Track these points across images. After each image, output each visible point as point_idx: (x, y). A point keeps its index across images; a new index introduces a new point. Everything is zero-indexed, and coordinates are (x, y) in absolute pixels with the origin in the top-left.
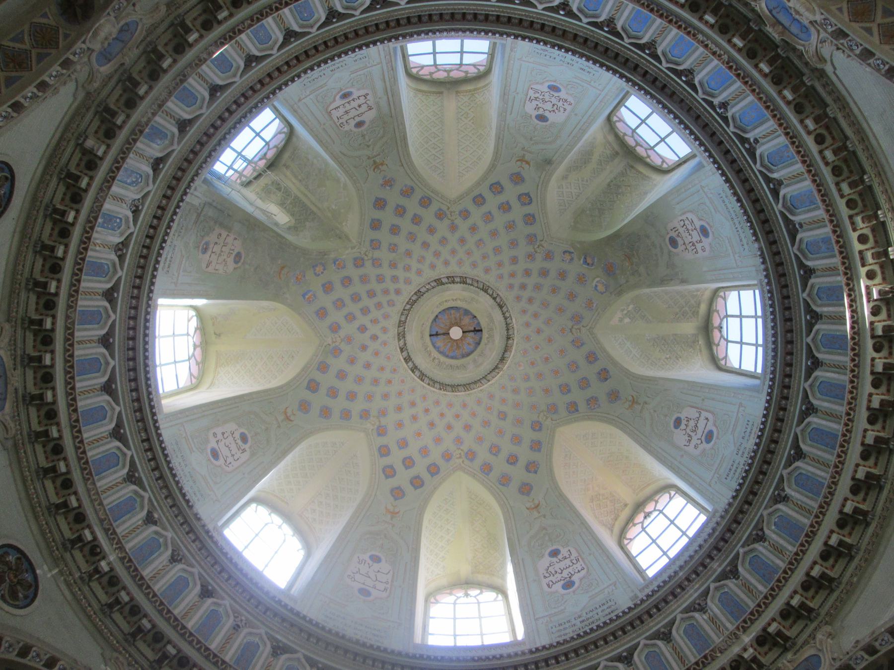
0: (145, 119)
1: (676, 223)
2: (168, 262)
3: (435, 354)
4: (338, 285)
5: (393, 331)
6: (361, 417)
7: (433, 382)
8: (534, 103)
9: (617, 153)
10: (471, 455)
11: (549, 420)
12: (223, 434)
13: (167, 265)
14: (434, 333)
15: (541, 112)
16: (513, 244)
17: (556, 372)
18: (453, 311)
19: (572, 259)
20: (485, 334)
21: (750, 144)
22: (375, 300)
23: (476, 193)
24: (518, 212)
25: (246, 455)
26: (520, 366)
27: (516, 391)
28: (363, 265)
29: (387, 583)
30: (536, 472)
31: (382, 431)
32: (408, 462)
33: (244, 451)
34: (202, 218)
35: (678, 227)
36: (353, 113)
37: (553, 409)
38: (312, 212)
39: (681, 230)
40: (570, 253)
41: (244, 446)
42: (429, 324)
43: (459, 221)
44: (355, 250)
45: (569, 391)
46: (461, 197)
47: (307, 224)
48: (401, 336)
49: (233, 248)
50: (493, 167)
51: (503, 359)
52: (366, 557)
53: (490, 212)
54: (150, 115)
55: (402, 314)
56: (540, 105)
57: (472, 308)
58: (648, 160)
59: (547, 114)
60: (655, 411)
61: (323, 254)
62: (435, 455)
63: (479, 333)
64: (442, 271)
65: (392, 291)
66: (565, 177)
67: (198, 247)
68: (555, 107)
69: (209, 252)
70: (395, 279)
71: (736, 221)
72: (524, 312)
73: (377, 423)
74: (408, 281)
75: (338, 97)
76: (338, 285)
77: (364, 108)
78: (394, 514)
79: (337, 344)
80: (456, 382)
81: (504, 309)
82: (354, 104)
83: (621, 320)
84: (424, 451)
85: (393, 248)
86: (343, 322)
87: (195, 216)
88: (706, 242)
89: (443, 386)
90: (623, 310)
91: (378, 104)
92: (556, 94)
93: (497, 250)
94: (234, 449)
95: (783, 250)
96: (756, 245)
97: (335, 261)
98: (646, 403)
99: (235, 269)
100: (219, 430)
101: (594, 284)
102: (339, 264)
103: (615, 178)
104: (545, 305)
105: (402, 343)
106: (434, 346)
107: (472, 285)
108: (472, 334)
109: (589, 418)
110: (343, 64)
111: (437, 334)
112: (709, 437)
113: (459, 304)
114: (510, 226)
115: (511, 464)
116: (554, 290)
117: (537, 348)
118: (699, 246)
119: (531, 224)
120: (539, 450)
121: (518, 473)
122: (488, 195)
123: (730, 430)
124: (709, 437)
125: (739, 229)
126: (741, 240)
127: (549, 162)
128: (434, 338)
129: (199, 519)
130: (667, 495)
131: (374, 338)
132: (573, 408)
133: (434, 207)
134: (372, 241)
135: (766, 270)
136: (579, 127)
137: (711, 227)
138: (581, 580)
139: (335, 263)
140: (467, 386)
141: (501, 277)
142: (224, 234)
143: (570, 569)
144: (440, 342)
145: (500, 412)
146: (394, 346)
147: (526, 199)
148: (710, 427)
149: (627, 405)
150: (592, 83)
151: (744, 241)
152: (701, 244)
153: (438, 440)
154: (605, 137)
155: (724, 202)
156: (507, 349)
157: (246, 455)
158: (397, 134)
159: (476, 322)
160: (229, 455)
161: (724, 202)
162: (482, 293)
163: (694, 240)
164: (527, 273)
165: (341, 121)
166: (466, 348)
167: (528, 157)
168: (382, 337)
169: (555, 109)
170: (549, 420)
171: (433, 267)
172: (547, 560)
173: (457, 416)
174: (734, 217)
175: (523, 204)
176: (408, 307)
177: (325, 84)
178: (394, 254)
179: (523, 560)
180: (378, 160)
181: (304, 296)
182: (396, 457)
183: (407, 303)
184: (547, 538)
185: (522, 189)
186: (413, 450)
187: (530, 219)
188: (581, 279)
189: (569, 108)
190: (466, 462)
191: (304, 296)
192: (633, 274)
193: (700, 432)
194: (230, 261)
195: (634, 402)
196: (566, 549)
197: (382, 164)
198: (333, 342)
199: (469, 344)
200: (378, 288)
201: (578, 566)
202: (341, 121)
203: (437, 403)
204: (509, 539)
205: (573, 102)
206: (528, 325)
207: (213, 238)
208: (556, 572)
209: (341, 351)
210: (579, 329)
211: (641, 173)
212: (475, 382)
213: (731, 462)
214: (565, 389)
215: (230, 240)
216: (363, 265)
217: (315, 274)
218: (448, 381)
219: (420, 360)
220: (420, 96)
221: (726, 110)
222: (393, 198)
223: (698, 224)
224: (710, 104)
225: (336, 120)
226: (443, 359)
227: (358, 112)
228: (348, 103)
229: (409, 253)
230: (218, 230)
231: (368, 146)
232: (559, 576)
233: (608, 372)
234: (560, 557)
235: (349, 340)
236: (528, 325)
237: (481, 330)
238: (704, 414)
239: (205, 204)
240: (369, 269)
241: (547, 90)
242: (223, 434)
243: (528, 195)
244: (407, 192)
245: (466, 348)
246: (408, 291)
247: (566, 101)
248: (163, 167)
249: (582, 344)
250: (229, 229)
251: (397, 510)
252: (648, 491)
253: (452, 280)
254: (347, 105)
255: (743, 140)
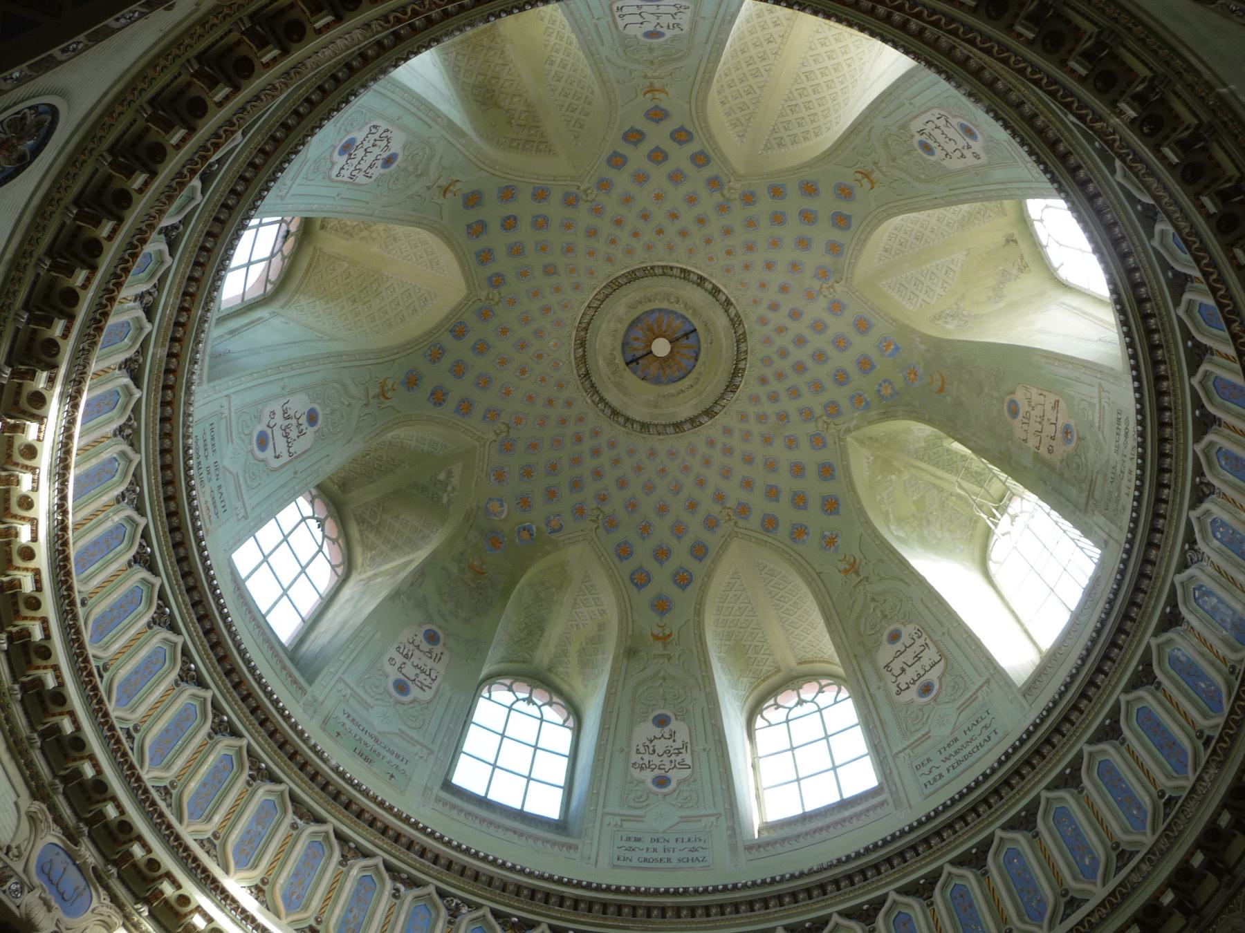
0: (1212, 771)
1: (440, 668)
2: (1123, 426)
3: (678, 308)
4: (853, 370)
5: (749, 323)
6: (753, 194)
7: (666, 271)
8: (678, 744)
9: (549, 670)
10: (571, 201)
11: (483, 298)
12: (963, 156)
13: (1123, 426)
14: (691, 336)
15: (666, 730)
16: (632, 506)
17: (503, 362)
18: (678, 374)
19: (548, 523)
20: (620, 361)
21: (403, 882)
22: (791, 360)
23: (708, 560)
24: (643, 555)
25: (917, 125)
26: (556, 345)
27: (547, 310)
28: (826, 407)
29: (622, 16)
30: (469, 227)
31: (715, 183)
32: (658, 156)
33: (921, 132)
34: (1085, 486)
35: (434, 665)
36: (909, 656)
37: (485, 314)
38: (921, 460)
39: (430, 663)
40: (554, 531)
41: (923, 138)
42: (703, 346)
43: (715, 509)
44: (844, 427)
45: (474, 348)
46: (724, 547)
47: (923, 445)
48: (736, 322)
49: (1025, 427)
50: (699, 612)
51: (582, 343)
52: (669, 34)
53: (679, 538)
54: (1206, 777)
55: (746, 352)
56: (670, 742)
57: (649, 391)
58: (508, 682)
59: (657, 731)
60: (350, 405)
61: (888, 415)
62: (622, 180)
63: (629, 359)
64: (711, 428)
65: (771, 379)
66: (601, 627)
67: (1079, 438)
68: (651, 749)
69: (1060, 424)
70: (774, 398)
71: (370, 742)
72: (580, 419)
73: (725, 192)
74: (755, 399)
75: (937, 686)
76: (853, 370)
77: (896, 666)
78: (651, 89)
79: (825, 286)
80: (634, 285)
81: (608, 411)
82: (911, 673)
83: (450, 474)
84: (641, 178)
85: (792, 443)
86: (827, 317)
87: (1097, 494)
88: (394, 674)
89: (649, 272)
90: (454, 489)
91: (880, 678)
92: (657, 772)
93: (649, 488)
94: (937, 133)
95: (298, 776)
96: (333, 762)
97: (868, 406)
98: (366, 405)
99: (1013, 393)
100: (970, 160)
101: (506, 508)
102: (858, 400)
103: (539, 641)
104: (557, 443)
105: (732, 312)
106: (683, 317)
107: (665, 426)
108: (639, 354)
109: (430, 333)
110: (945, 754)
111: (686, 335)
112: (263, 442)
113: (672, 389)
114: (645, 530)
115: (509, 218)
116: (553, 468)
117: (543, 380)
118: (399, 659)
119: (619, 545)
120: (478, 254)
121: (493, 212)
122: (691, 564)
123: (241, 478)
124: (263, 442)
125: (360, 734)
126: (353, 720)
127: (630, 652)
128: (688, 328)
129: (970, 95)
130: (273, 277)
131: (774, 307)
132: (459, 331)
133: (756, 518)
134: (824, 446)
135: (306, 741)
136: (612, 729)
137: (398, 702)
138: (333, 164)
139: (868, 404)
140: (615, 286)
141: (631, 452)
142: (1043, 451)
143: (355, 162)
144: (679, 327)
145: (555, 273)
146: (741, 304)
147: (640, 580)
148: (269, 453)
149: (390, 383)
150: (618, 819)
151: (349, 724)
152: (398, 665)
153: (627, 200)
154: (572, 687)
155: (397, 756)
156: (583, 360)
157: (917, 125)
158: (840, 627)
159: (639, 372)
160: (943, 128)
161: (397, 756)
162: (647, 420)
163: (409, 663)
164: (598, 474)
165: (921, 641)
166: (638, 333)
167: (658, 648)
168: (762, 310)
169: (649, 747)
170: (483, 298)
171: (728, 431)
172: (395, 147)
173: (613, 242)
174: (377, 747)
175: (640, 570)
176: (741, 365)
177: (961, 710)
178: (787, 434)
179: (431, 127)
180: (855, 579)
181: (897, 349)
182: (680, 157)
183: (744, 370)
184: (411, 169)
185: (649, 592)
186: (658, 176)
187: (624, 552)
188: (525, 503)
189: (635, 758)
190: (574, 190)
191: (897, 349)
192: (462, 554)
193: (278, 433)
194: (1024, 408)
195: (383, 394)
196: (374, 177)
197: (846, 571)
198: (832, 287)
199: (637, 339)
200: (794, 379)
201: (346, 173)
202: (921, 641)
203: (649, 247)
204: (464, 134)
205: (633, 770)
206: (569, 404)
207: (1061, 450)
208: (374, 145)
209: (816, 276)
210: (498, 435)
211: (510, 662)
212: (607, 296)
213: (217, 447)
214: (481, 348)
215: (1032, 442)
216: (826, 407)
217: (890, 383)
218: (647, 282)
219: (697, 296)
220: (826, 656)
221: (448, 909)
222: (814, 518)
223: (415, 692)
224: (470, 904)
225: (928, 641)
226: (665, 305)
227: (902, 659)
228: (920, 676)
229: (767, 440)
230: (1056, 458)
231: (873, 600)
232: (366, 145)
233: (435, 404)
234: (379, 163)
235: (810, 295)
236: (569, 404)
237: (627, 364)
238: (285, 458)
239: (1086, 511)
240: (816, 403)
241: (670, 774)
242: (963, 156)
243: (640, 586)
244: (799, 532)
245: (638, 333)
246: (748, 385)
247: (642, 768)
248: (1164, 609)
249: (484, 417)
250: (1037, 457)
251: (649, 95)
252: (304, 262)
253: (693, 421)
254: (922, 672)
255: (412, 883)
